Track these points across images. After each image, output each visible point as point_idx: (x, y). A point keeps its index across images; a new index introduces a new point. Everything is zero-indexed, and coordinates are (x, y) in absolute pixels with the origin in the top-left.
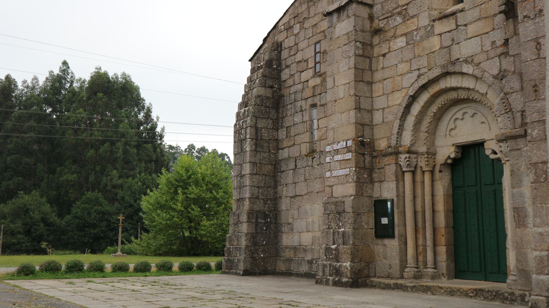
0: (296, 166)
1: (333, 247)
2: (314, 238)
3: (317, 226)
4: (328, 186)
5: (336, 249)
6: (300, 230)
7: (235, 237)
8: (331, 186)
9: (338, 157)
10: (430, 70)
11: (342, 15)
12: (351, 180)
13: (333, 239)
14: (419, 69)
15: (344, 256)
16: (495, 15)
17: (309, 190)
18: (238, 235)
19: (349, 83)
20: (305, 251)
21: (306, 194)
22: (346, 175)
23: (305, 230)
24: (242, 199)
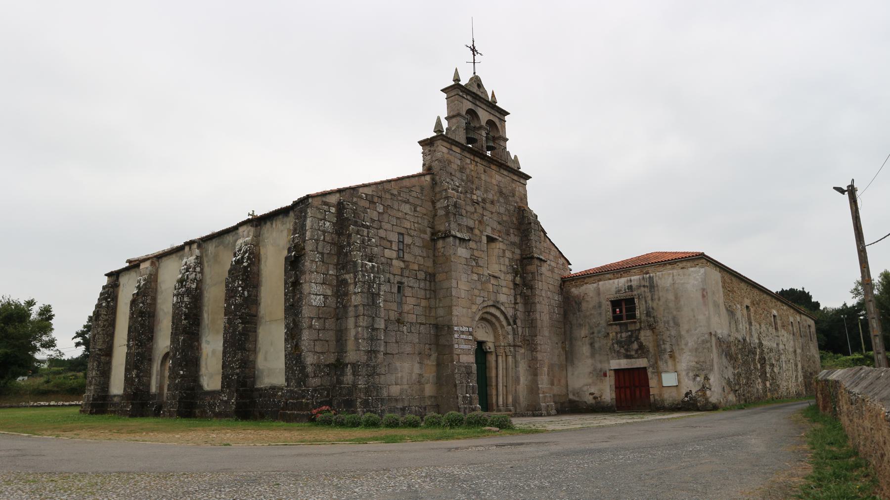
0: (386, 328)
1: (468, 395)
2: (402, 391)
3: (405, 381)
4: (456, 354)
5: (470, 397)
6: (389, 383)
7: (374, 388)
8: (458, 355)
9: (464, 337)
10: (488, 300)
11: (462, 243)
12: (472, 353)
13: (466, 391)
14: (483, 297)
15: (475, 401)
16: (511, 289)
17: (400, 351)
18: (378, 387)
19: (468, 291)
20: (396, 400)
21: (396, 354)
22: (469, 349)
23: (394, 383)
24: (374, 351)
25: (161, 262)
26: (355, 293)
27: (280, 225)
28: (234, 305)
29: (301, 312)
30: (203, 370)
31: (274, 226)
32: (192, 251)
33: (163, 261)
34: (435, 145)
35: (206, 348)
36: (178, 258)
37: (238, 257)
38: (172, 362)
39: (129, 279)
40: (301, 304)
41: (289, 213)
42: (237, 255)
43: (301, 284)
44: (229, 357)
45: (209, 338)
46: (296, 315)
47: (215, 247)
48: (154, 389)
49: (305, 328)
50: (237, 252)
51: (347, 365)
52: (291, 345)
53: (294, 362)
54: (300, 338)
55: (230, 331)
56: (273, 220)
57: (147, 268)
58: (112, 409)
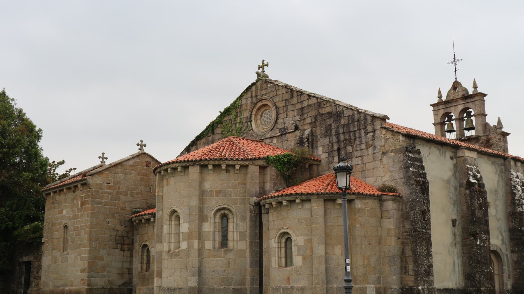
36: (490, 163)
39: (429, 154)
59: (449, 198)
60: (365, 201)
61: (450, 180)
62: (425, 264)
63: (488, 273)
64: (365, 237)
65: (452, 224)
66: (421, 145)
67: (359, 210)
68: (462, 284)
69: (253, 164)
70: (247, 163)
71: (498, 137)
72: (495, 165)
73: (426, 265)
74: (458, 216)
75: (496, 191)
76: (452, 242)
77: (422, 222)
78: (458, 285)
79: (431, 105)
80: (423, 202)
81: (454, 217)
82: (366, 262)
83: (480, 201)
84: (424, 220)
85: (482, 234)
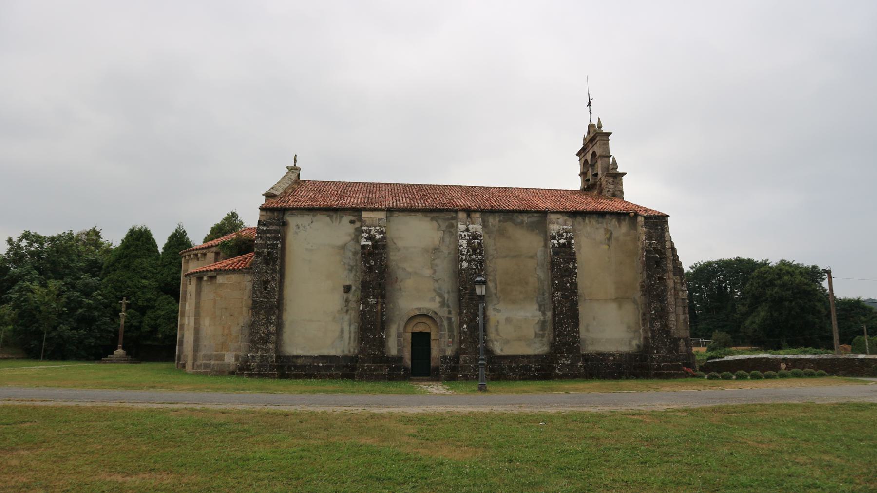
25: (390, 216)
26: (682, 290)
27: (594, 223)
28: (569, 283)
29: (667, 300)
30: (492, 335)
31: (587, 221)
32: (473, 219)
33: (395, 215)
34: (618, 179)
35: (495, 315)
36: (428, 219)
37: (562, 242)
38: (468, 327)
39: (312, 222)
40: (667, 294)
41: (605, 216)
42: (558, 239)
43: (665, 279)
44: (567, 327)
45: (497, 307)
46: (662, 302)
47: (500, 221)
48: (393, 349)
49: (671, 312)
50: (557, 237)
51: (679, 339)
52: (660, 322)
53: (664, 336)
54: (668, 319)
55: (566, 305)
56: (585, 217)
57: (380, 220)
58: (294, 372)
59: (342, 263)
60: (227, 276)
61: (345, 245)
62: (261, 332)
63: (374, 339)
64: (226, 309)
65: (343, 291)
66: (299, 215)
67: (221, 285)
68: (354, 352)
69: (209, 252)
70: (204, 251)
71: (606, 180)
72: (437, 221)
73: (263, 333)
74: (356, 281)
75: (436, 250)
76: (342, 309)
77: (261, 293)
78: (346, 352)
79: (577, 155)
80: (266, 272)
81: (348, 283)
82: (226, 332)
83: (369, 264)
84: (265, 289)
85: (369, 298)
